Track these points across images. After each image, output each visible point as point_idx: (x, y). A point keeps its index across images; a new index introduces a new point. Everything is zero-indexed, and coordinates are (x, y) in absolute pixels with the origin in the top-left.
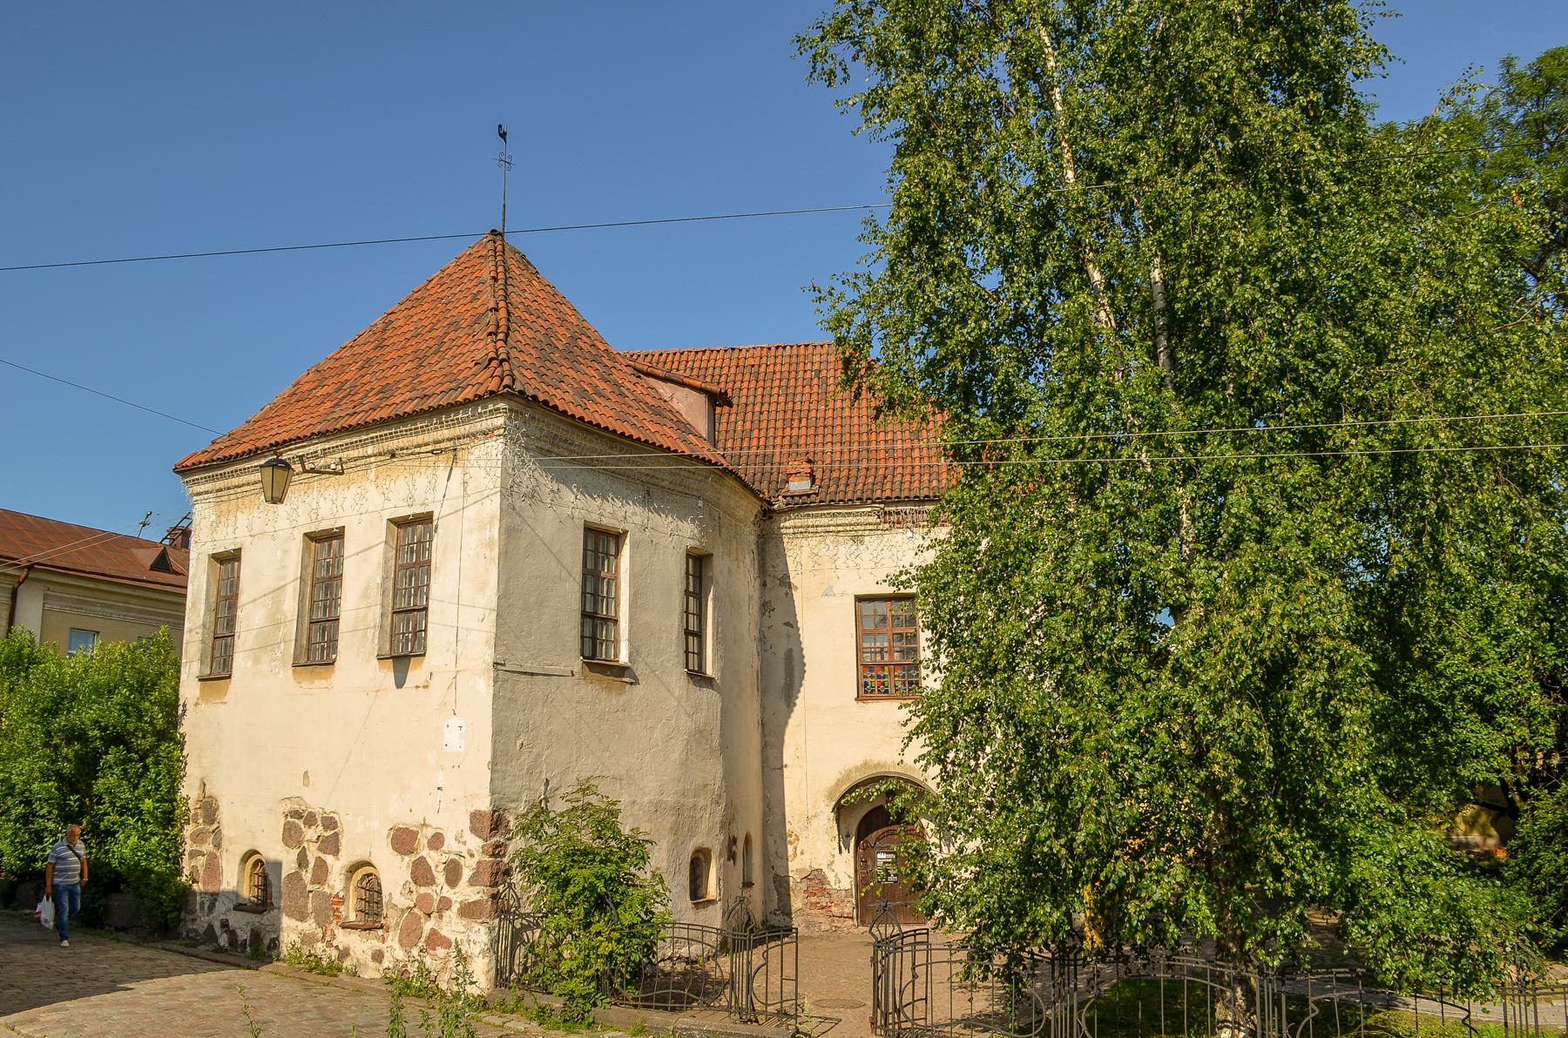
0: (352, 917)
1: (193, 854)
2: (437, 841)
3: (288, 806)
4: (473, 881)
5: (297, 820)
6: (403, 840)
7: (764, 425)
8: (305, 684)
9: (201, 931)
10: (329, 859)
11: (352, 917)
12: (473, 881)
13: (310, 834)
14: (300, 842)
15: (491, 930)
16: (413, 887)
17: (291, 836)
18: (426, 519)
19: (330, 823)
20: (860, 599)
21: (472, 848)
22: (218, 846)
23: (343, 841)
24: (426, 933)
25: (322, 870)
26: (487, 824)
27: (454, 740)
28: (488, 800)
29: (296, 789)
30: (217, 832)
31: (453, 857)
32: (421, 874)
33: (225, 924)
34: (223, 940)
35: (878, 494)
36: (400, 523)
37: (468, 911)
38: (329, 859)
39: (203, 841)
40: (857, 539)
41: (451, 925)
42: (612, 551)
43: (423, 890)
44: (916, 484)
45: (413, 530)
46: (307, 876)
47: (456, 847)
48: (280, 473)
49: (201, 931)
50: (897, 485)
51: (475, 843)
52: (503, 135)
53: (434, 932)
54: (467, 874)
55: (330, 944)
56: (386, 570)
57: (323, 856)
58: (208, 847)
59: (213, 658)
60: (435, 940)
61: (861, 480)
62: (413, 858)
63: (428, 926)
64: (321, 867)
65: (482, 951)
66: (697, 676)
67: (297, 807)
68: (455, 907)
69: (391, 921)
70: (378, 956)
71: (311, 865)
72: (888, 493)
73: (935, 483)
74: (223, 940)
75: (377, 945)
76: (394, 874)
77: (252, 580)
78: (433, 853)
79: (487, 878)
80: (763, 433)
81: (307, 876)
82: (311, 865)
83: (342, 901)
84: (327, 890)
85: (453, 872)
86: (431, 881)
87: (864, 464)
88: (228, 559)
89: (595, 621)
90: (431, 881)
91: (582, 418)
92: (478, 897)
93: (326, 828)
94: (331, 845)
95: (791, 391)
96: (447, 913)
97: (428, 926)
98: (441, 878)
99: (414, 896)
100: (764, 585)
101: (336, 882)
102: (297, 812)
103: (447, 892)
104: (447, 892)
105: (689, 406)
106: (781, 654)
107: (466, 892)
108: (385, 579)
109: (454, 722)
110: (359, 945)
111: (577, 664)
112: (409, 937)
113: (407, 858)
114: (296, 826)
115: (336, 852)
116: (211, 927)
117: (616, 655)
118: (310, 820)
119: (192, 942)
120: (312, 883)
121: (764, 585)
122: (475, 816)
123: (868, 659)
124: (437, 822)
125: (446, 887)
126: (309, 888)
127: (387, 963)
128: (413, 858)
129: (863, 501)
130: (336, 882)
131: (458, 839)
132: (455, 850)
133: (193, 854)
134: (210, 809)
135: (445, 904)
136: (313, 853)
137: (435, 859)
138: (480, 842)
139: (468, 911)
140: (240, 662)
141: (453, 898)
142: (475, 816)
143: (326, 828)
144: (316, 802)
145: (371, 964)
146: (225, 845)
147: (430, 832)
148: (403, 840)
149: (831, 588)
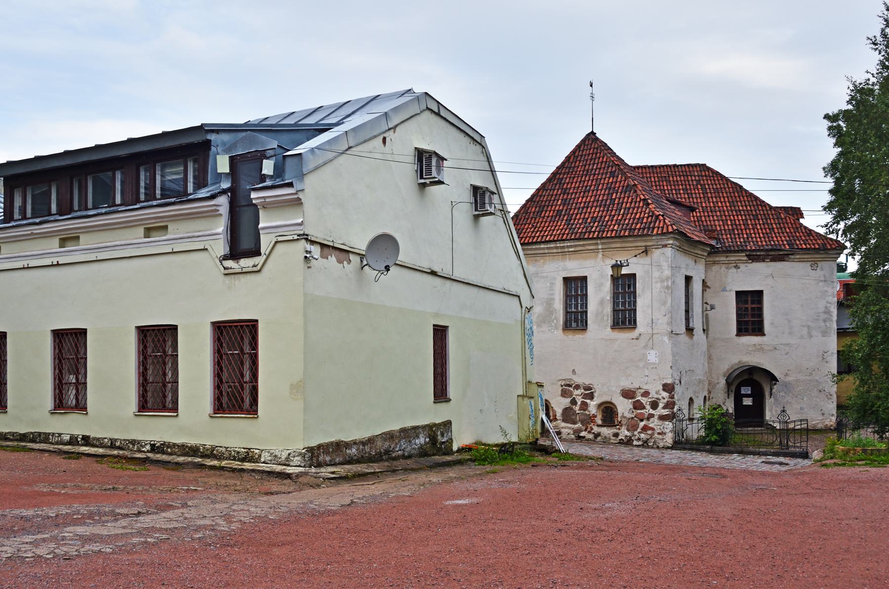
0: (600, 422)
4: (664, 408)
6: (628, 394)
8: (570, 336)
10: (588, 401)
12: (664, 408)
13: (578, 392)
17: (564, 394)
23: (596, 394)
25: (584, 406)
27: (652, 357)
29: (569, 375)
32: (638, 406)
37: (662, 418)
40: (737, 267)
41: (654, 423)
43: (639, 411)
47: (656, 396)
51: (665, 394)
52: (591, 86)
53: (645, 425)
54: (661, 405)
55: (589, 432)
63: (642, 424)
68: (656, 417)
75: (615, 430)
76: (624, 407)
82: (579, 403)
83: (595, 416)
84: (587, 412)
85: (654, 405)
86: (644, 408)
90: (644, 408)
94: (591, 396)
97: (642, 424)
98: (648, 407)
103: (651, 411)
104: (651, 411)
107: (661, 411)
109: (653, 352)
110: (606, 431)
112: (632, 427)
118: (577, 387)
124: (645, 387)
127: (620, 438)
129: (742, 251)
131: (657, 393)
135: (651, 416)
136: (579, 400)
137: (644, 400)
143: (585, 390)
144: (578, 380)
147: (642, 391)
148: (628, 394)
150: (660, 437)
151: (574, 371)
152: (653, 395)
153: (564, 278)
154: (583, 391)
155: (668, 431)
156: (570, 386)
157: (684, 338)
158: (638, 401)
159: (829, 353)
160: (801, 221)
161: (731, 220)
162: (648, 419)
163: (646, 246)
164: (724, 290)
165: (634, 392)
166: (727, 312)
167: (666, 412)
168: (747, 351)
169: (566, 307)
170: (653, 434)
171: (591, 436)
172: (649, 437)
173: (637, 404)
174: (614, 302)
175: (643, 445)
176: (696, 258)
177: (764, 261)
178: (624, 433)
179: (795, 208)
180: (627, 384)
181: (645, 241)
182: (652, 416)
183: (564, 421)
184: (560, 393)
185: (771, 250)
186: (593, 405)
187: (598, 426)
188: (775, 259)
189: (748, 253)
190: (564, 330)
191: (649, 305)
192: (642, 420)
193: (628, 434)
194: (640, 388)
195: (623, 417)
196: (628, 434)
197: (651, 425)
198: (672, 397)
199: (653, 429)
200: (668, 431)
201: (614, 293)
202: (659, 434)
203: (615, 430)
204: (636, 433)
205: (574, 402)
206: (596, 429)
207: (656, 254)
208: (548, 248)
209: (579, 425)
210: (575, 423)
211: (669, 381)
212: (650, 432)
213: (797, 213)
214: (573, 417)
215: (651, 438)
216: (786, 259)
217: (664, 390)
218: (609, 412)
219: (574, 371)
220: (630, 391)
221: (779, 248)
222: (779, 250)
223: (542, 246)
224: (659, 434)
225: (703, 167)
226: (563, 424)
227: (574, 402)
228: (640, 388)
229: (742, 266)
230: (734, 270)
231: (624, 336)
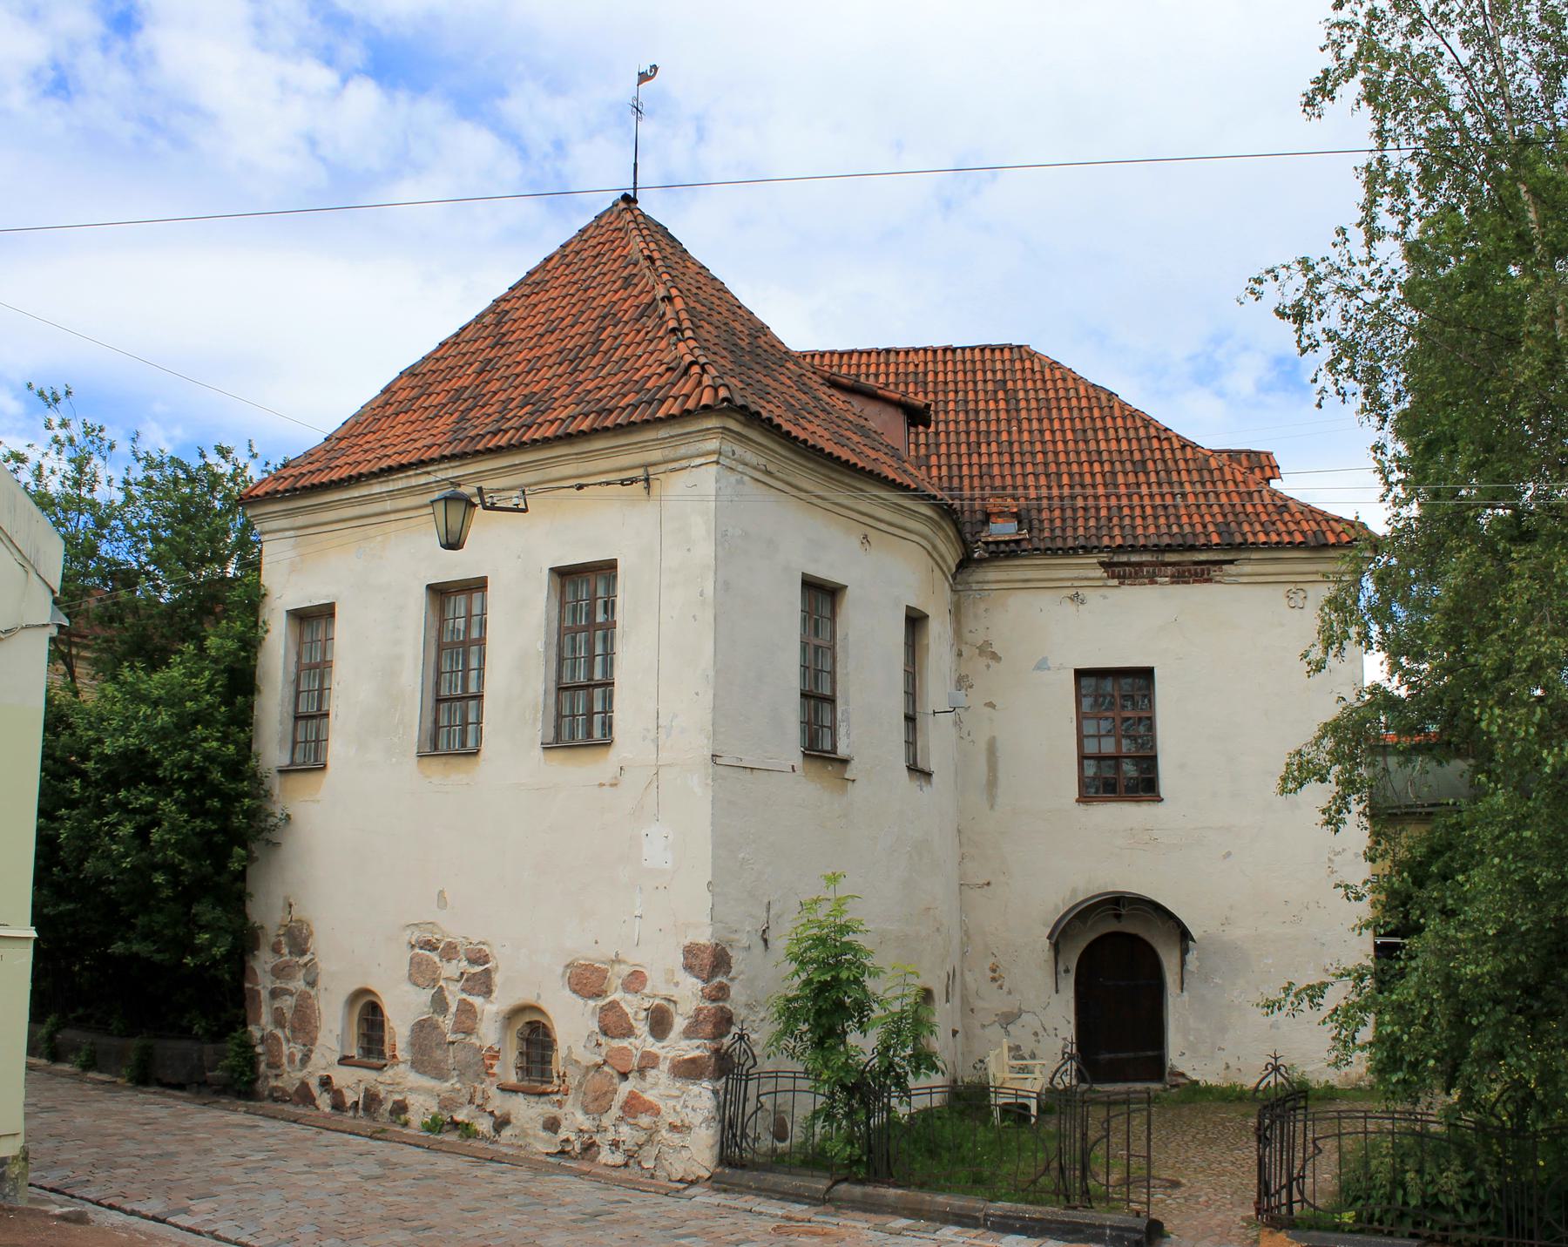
0: (513, 1078)
1: (275, 994)
2: (635, 981)
3: (416, 936)
4: (689, 1033)
5: (429, 950)
6: (586, 981)
7: (943, 449)
9: (291, 1090)
10: (477, 1001)
11: (513, 1078)
12: (689, 1033)
13: (450, 969)
14: (435, 981)
15: (715, 1092)
16: (603, 1040)
17: (420, 973)
18: (607, 569)
19: (479, 958)
20: (1080, 674)
21: (688, 994)
22: (312, 984)
23: (497, 978)
24: (619, 1099)
26: (707, 959)
27: (656, 850)
28: (709, 931)
30: (310, 967)
31: (657, 1001)
32: (613, 1024)
33: (326, 1083)
34: (324, 1101)
35: (1106, 541)
36: (565, 576)
37: (688, 1070)
38: (477, 1001)
39: (290, 977)
40: (1075, 598)
41: (659, 1088)
42: (827, 612)
44: (1152, 530)
45: (584, 588)
46: (447, 1023)
48: (456, 511)
49: (291, 1090)
50: (1128, 530)
53: (633, 1097)
54: (679, 1023)
56: (547, 633)
57: (471, 999)
58: (298, 984)
59: (295, 743)
60: (634, 1106)
61: (1080, 522)
62: (602, 1002)
63: (625, 1088)
64: (466, 1010)
65: (706, 1120)
66: (918, 771)
67: (428, 936)
68: (665, 1066)
69: (573, 1081)
70: (552, 1125)
71: (453, 1009)
72: (1119, 541)
73: (1175, 529)
74: (324, 1101)
76: (573, 1026)
77: (348, 643)
78: (629, 997)
79: (709, 1028)
80: (943, 460)
81: (447, 1023)
82: (453, 1009)
85: (659, 1022)
86: (629, 1032)
87: (1080, 503)
88: (314, 620)
89: (818, 701)
90: (629, 1032)
91: (805, 441)
92: (697, 1053)
93: (472, 962)
94: (482, 984)
95: (971, 406)
96: (653, 1072)
97: (625, 1088)
98: (642, 1028)
99: (604, 1050)
100: (960, 654)
101: (489, 1033)
102: (428, 942)
105: (888, 423)
106: (982, 745)
107: (680, 1046)
108: (547, 645)
110: (526, 1112)
111: (796, 758)
112: (598, 1103)
113: (591, 1003)
114: (429, 962)
115: (487, 992)
116: (304, 1085)
117: (834, 746)
118: (450, 952)
119: (278, 1097)
120: (455, 1032)
121: (960, 654)
122: (691, 951)
123: (1091, 747)
125: (651, 1040)
126: (450, 1037)
127: (563, 1134)
128: (602, 1002)
129: (1087, 550)
130: (489, 1033)
132: (664, 993)
133: (275, 994)
134: (297, 939)
135: (649, 1062)
137: (634, 1006)
138: (700, 984)
139: (688, 1070)
140: (337, 749)
141: (662, 1053)
142: (691, 951)
144: (453, 929)
145: (543, 1134)
146: (321, 984)
147: (625, 970)
148: (586, 981)
149: (1045, 660)
150: (676, 1138)
151: (441, 893)
152: (657, 986)
153: (431, 588)
154: (464, 963)
155: (696, 1119)
156: (430, 945)
157: (807, 791)
158: (614, 1005)
159: (1349, 855)
160: (1274, 484)
161: (1071, 475)
162: (642, 1071)
163: (646, 466)
164: (1042, 666)
165: (603, 975)
166: (1048, 733)
167: (693, 1049)
168: (1114, 851)
169: (438, 684)
170: (652, 1132)
171: (484, 1125)
172: (642, 1137)
173: (612, 1018)
174: (561, 660)
175: (626, 1165)
176: (869, 530)
177: (1153, 582)
178: (575, 1119)
179: (1257, 453)
180: (585, 942)
181: (643, 446)
182: (649, 1062)
183: (418, 1065)
184: (405, 969)
185: (1169, 548)
186: (490, 1010)
187: (504, 1089)
188: (1183, 576)
189: (1104, 557)
190: (421, 756)
191: (664, 665)
192: (624, 1076)
193: (584, 1122)
194: (617, 960)
195: (570, 1060)
196: (584, 1122)
197: (650, 1096)
198: (721, 993)
199: (654, 1110)
200: (696, 1119)
201: (562, 632)
202: (673, 1128)
203: (543, 1108)
204: (607, 1121)
205: (439, 1003)
206: (498, 1103)
207: (675, 486)
208: (391, 494)
209: (453, 1082)
210: (441, 1076)
211: (704, 937)
212: (645, 1120)
213: (1261, 465)
214: (438, 1054)
215: (649, 1140)
216: (1215, 572)
217: (688, 967)
218: (536, 1039)
219: (441, 893)
220: (588, 967)
221: (1190, 541)
222: (1192, 548)
223: (377, 488)
224: (673, 1128)
225: (1021, 353)
226: (414, 1079)
227: (439, 1003)
228: (617, 960)
229: (1090, 595)
230: (1070, 608)
231: (579, 772)
